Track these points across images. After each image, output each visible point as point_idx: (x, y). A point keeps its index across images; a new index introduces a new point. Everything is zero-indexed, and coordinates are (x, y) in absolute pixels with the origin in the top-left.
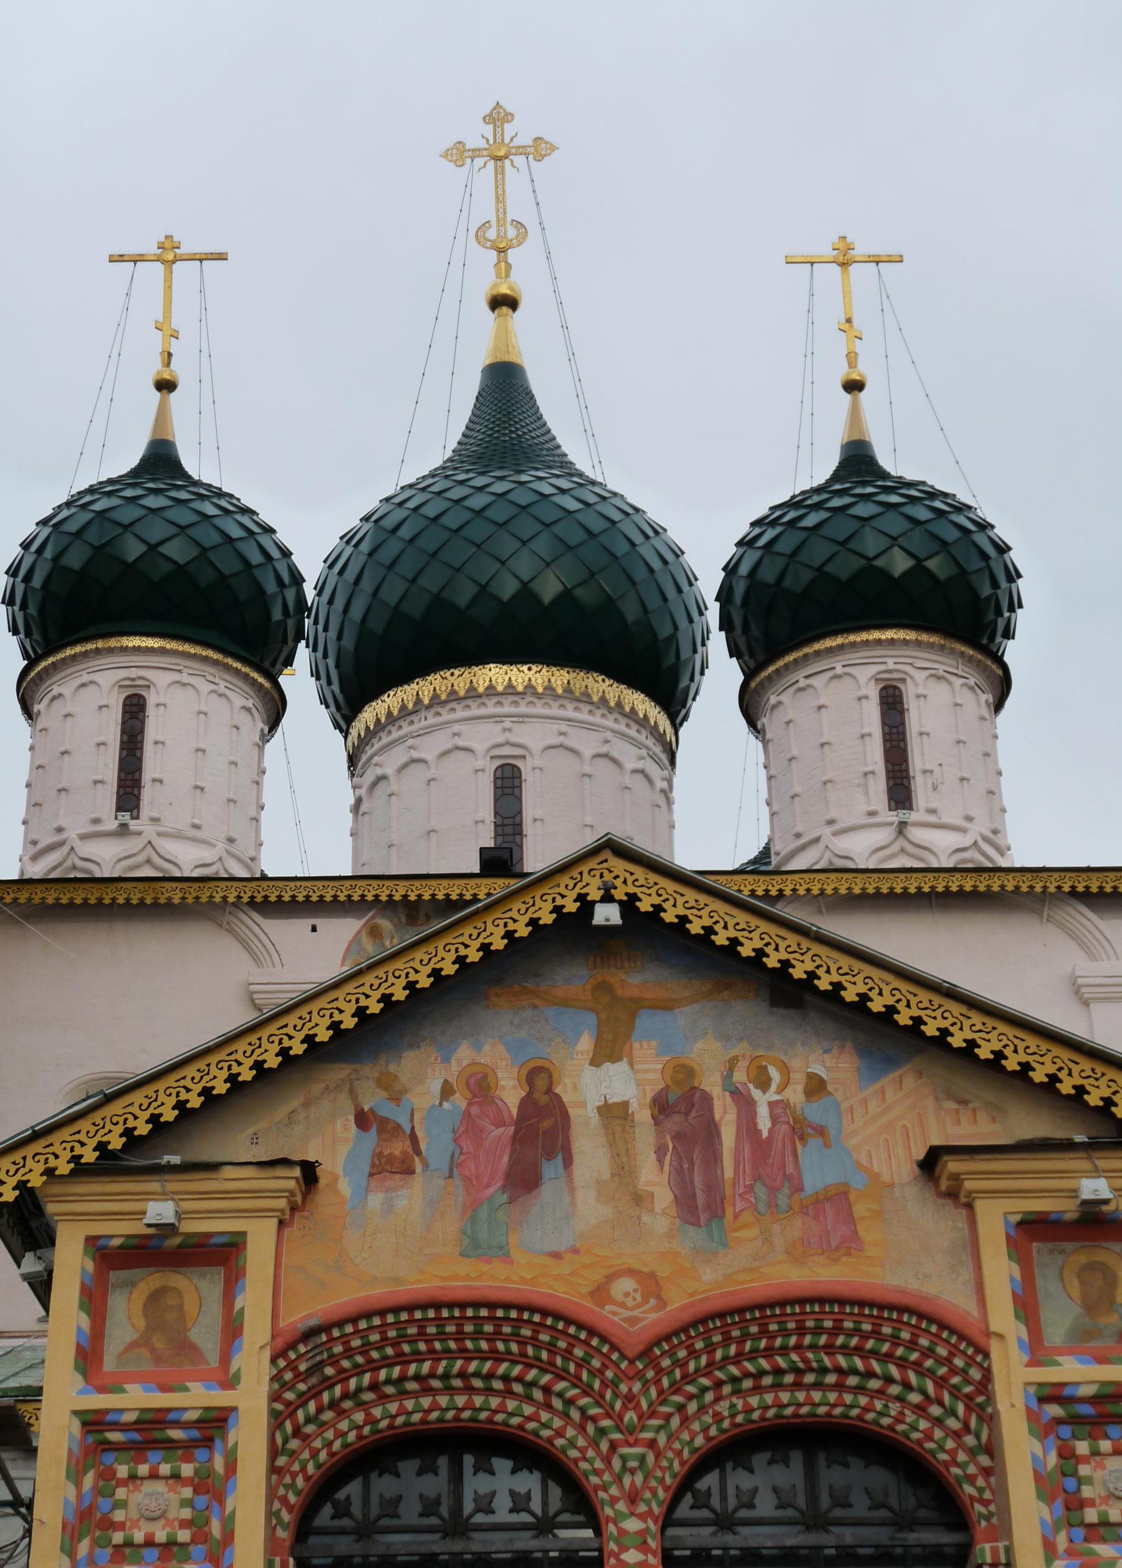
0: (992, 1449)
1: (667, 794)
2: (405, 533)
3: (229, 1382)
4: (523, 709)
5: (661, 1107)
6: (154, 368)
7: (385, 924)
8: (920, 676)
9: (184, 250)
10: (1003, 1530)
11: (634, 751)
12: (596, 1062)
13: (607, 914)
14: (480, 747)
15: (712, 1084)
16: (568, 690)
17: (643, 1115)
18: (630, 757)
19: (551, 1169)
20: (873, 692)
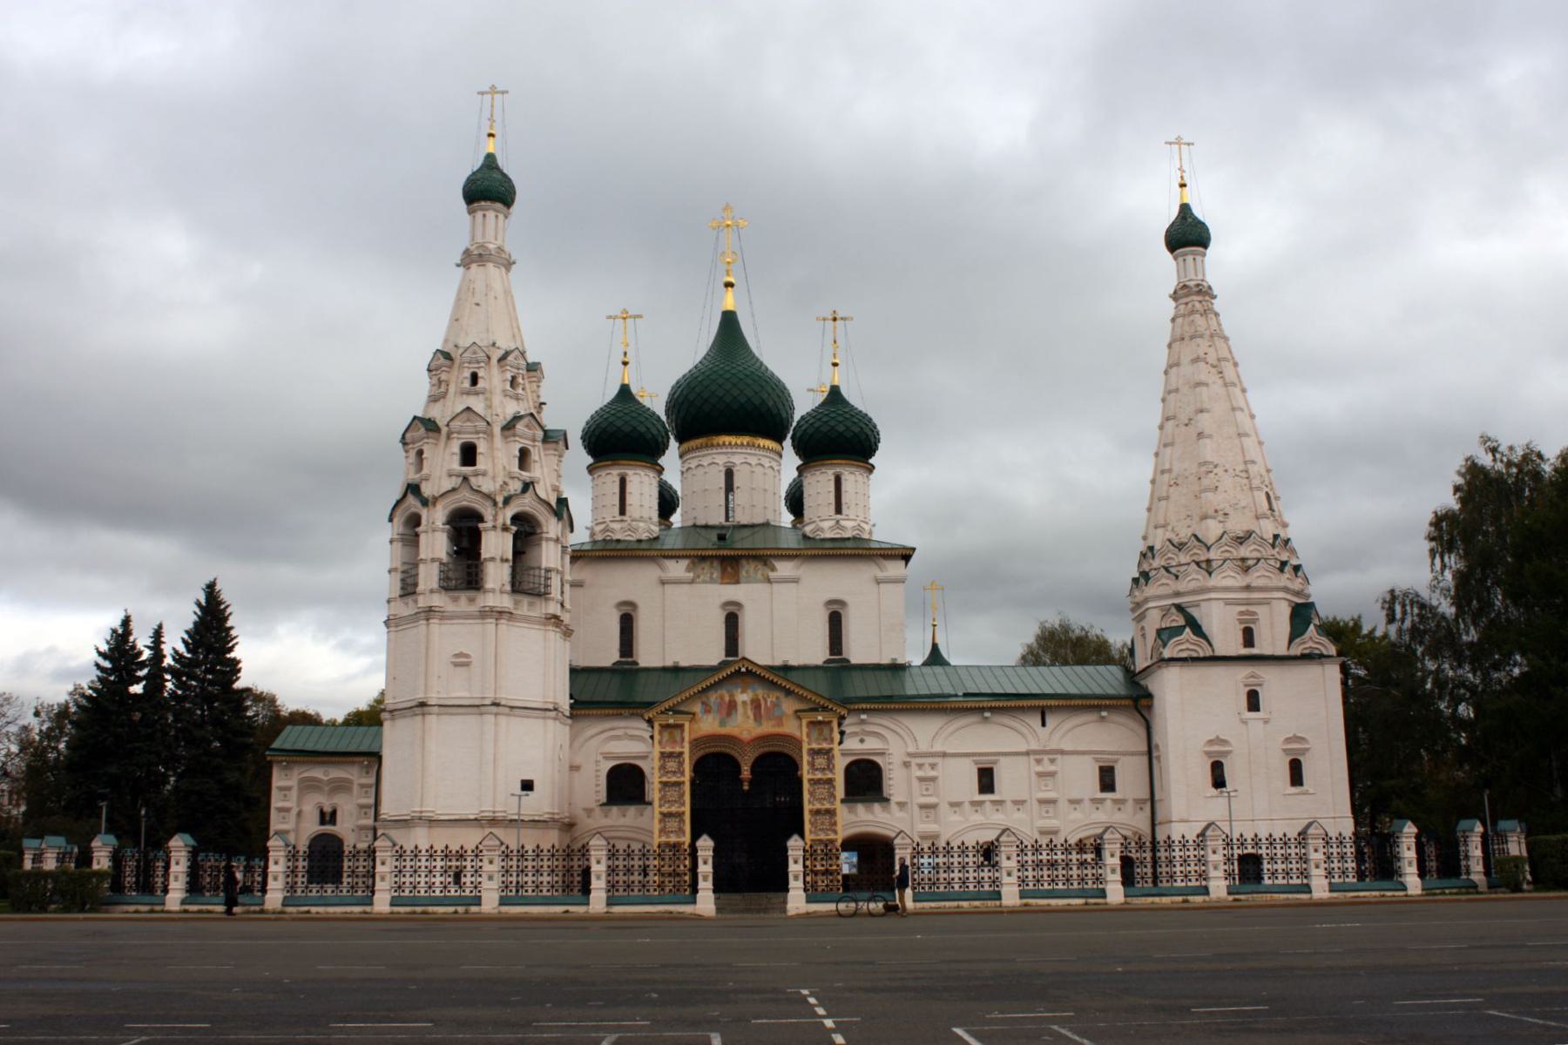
0: (802, 757)
1: (779, 471)
2: (699, 379)
3: (683, 747)
4: (734, 450)
5: (753, 701)
6: (621, 358)
7: (696, 560)
8: (846, 473)
9: (630, 313)
10: (802, 769)
11: (768, 460)
12: (743, 692)
13: (743, 670)
14: (721, 463)
15: (760, 697)
16: (748, 444)
17: (749, 702)
18: (766, 462)
19: (734, 712)
20: (833, 478)
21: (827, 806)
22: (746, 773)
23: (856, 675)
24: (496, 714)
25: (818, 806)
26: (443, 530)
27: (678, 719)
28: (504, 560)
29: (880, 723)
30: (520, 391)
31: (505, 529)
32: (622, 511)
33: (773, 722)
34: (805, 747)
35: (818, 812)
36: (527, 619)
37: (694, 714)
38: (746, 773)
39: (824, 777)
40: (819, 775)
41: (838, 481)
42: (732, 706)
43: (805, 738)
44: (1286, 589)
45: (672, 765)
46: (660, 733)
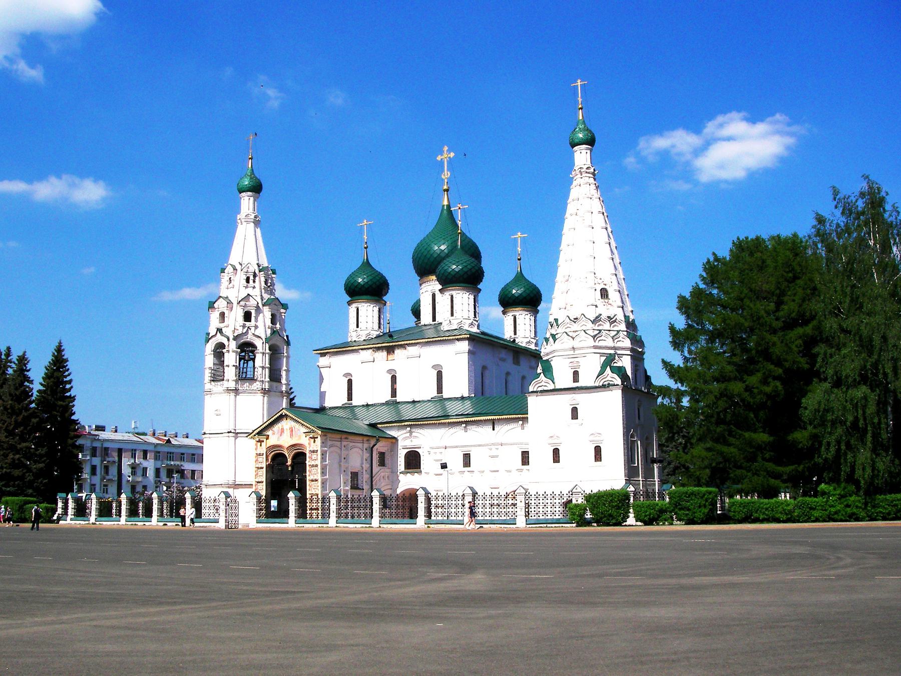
13: (284, 414)
21: (315, 477)
22: (289, 463)
23: (448, 403)
24: (229, 437)
25: (312, 477)
26: (211, 354)
27: (262, 438)
28: (228, 366)
29: (418, 432)
30: (251, 281)
31: (233, 351)
32: (358, 327)
33: (297, 438)
34: (308, 449)
35: (312, 481)
36: (244, 392)
37: (268, 436)
38: (289, 463)
39: (315, 464)
40: (313, 463)
41: (452, 297)
42: (282, 431)
43: (307, 445)
44: (595, 347)
45: (260, 459)
46: (256, 445)
